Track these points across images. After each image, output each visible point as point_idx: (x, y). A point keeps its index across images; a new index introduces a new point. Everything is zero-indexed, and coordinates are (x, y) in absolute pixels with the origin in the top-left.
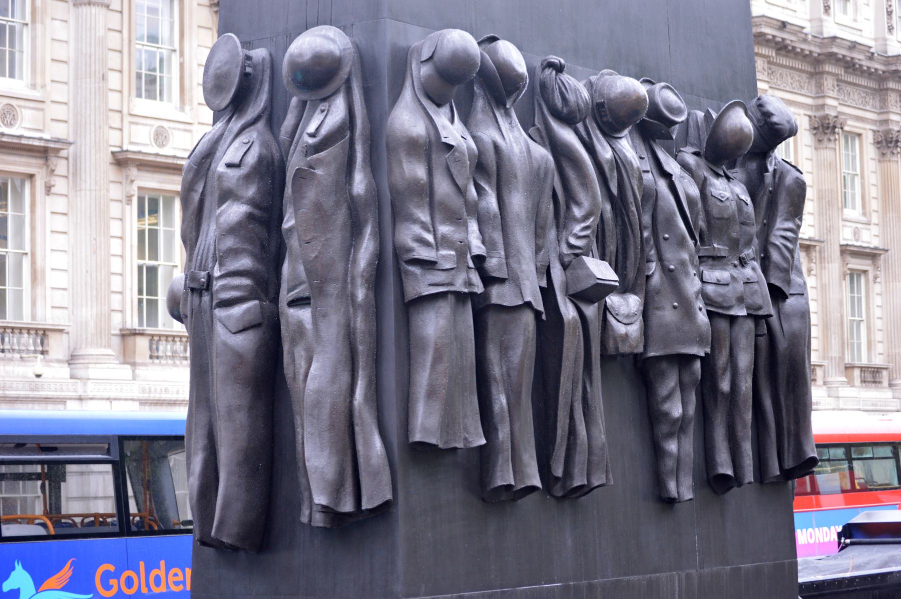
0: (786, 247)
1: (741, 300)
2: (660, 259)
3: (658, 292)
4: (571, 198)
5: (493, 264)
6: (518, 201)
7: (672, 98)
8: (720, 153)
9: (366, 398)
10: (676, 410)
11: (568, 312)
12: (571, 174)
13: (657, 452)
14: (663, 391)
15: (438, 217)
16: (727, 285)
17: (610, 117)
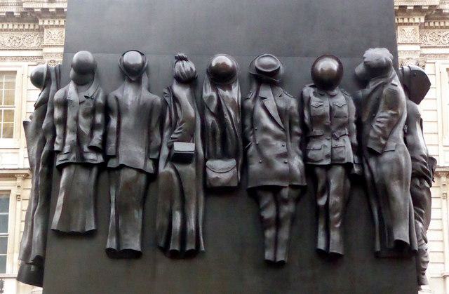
0: (378, 127)
1: (327, 156)
2: (255, 141)
3: (251, 156)
4: (177, 117)
5: (111, 149)
6: (127, 121)
7: (267, 60)
8: (325, 84)
9: (38, 213)
10: (269, 214)
11: (164, 168)
12: (177, 104)
13: (263, 237)
14: (261, 206)
15: (68, 131)
16: (320, 149)
17: (221, 77)
